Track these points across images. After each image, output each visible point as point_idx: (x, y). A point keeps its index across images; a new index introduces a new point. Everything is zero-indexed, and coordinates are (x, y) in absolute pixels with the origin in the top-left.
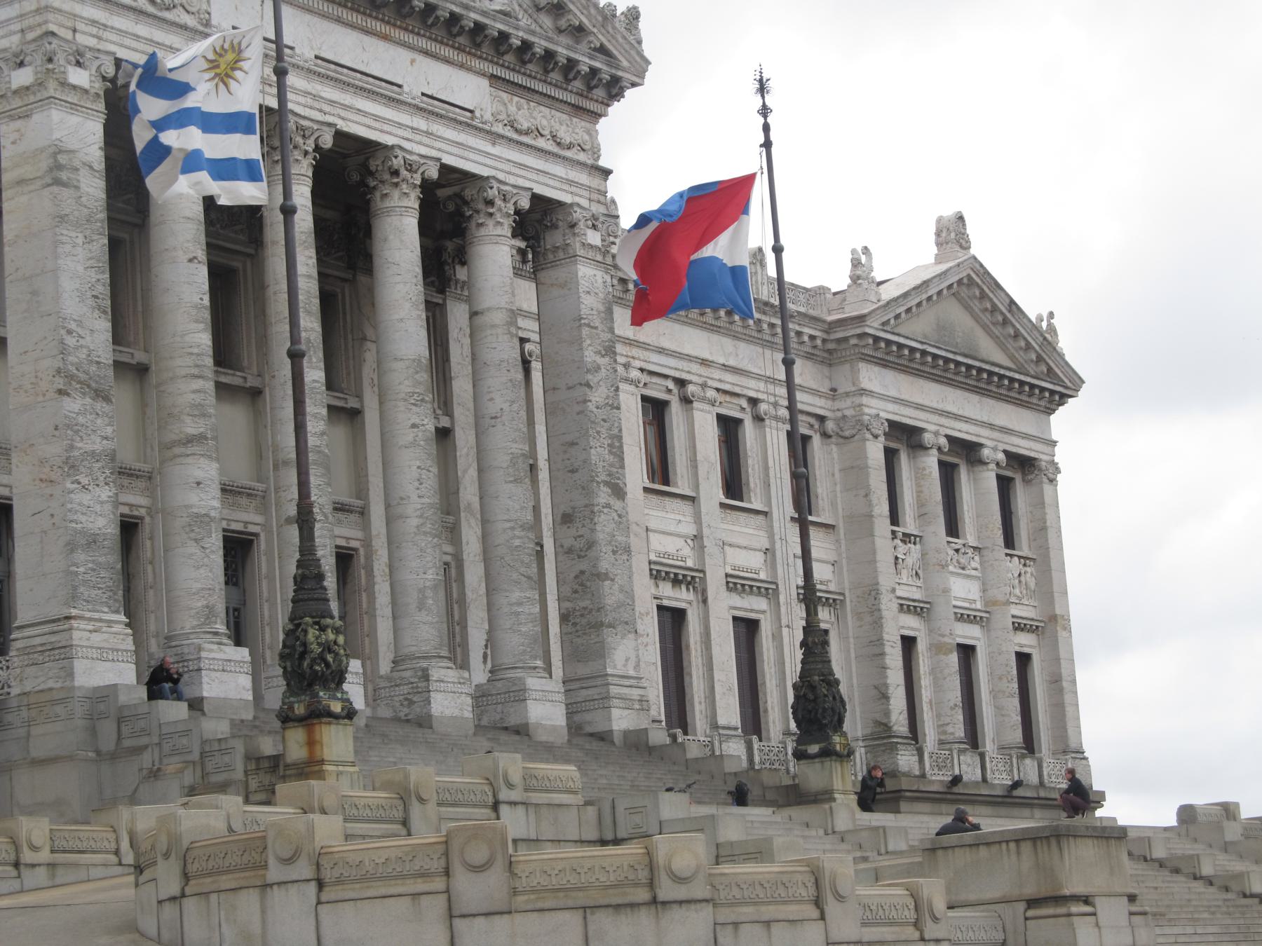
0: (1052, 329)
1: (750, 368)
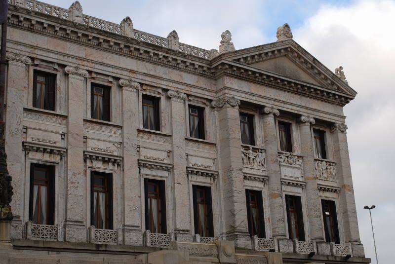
0: (342, 74)
1: (164, 76)
